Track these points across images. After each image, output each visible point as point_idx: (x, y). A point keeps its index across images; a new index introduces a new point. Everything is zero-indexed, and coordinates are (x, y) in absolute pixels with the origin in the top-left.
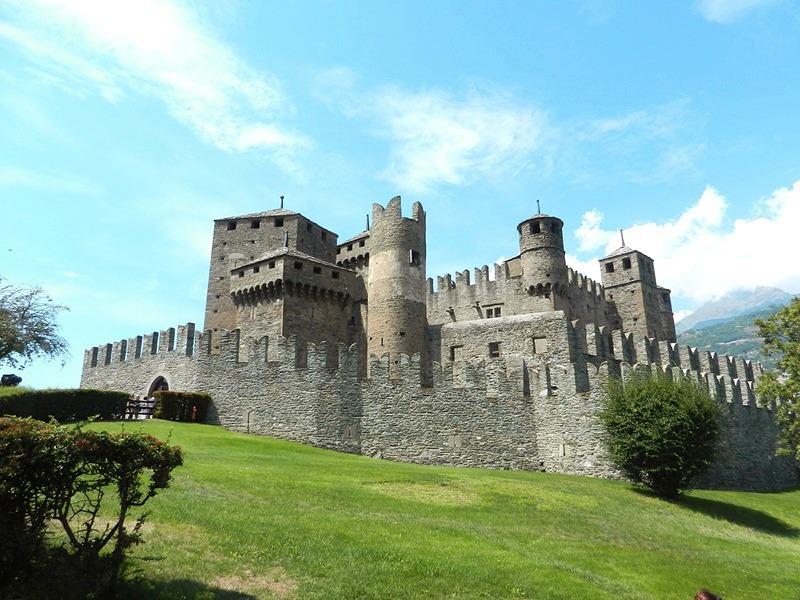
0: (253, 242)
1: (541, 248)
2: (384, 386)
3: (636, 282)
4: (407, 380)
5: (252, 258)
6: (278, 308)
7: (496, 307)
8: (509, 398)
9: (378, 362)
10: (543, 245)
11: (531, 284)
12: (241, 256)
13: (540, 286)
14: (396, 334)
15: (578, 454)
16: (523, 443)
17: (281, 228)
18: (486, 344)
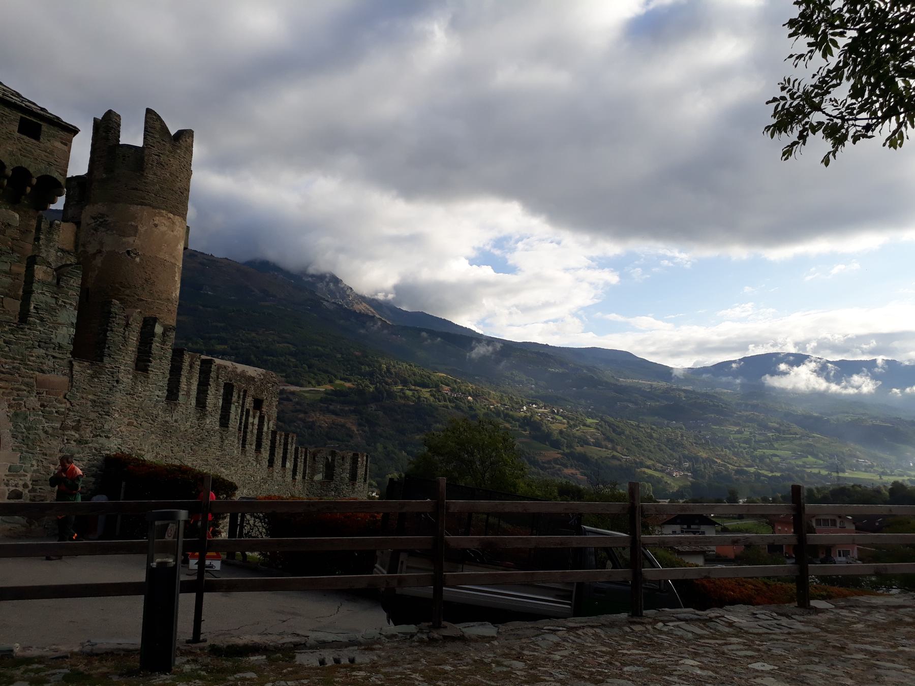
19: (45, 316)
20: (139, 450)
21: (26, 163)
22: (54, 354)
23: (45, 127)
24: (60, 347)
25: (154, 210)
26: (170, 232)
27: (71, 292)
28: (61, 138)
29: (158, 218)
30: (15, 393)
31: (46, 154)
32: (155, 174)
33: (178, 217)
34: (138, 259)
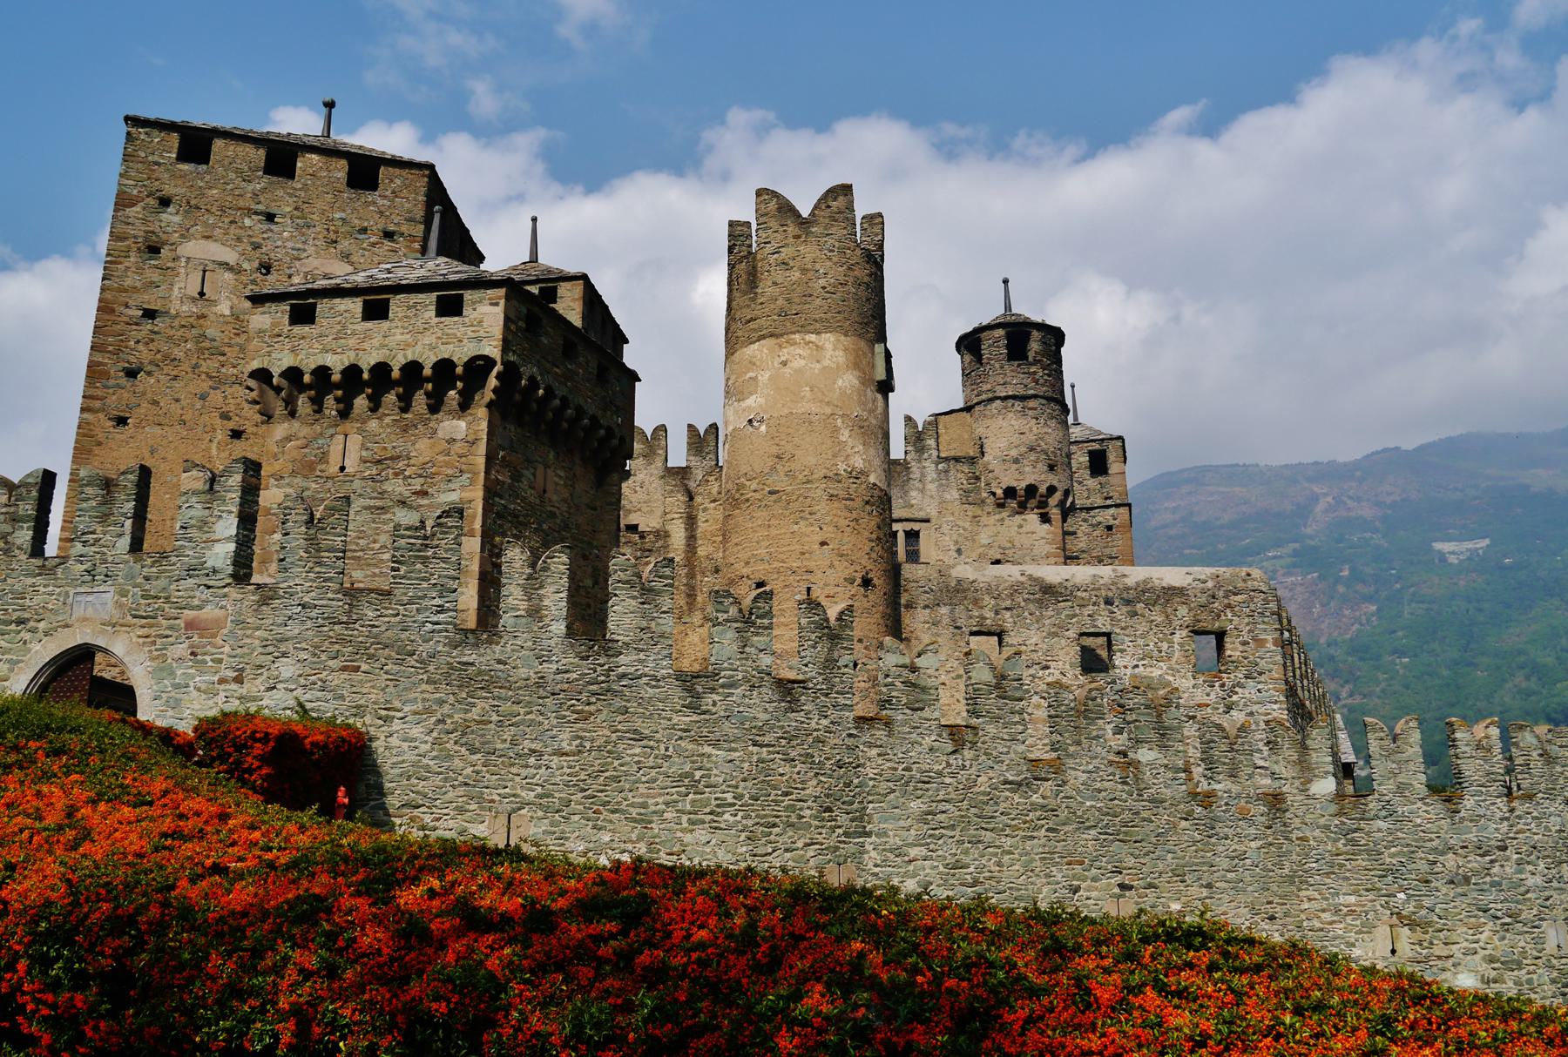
0: (270, 218)
1: (1035, 396)
2: (928, 741)
3: (1117, 506)
4: (991, 729)
5: (266, 268)
6: (457, 448)
7: (909, 526)
8: (1238, 796)
9: (914, 669)
10: (1042, 390)
11: (1008, 480)
12: (231, 256)
13: (1031, 490)
14: (851, 581)
15: (1438, 953)
16: (1272, 918)
17: (370, 196)
18: (1072, 634)
19: (194, 533)
20: (385, 709)
21: (445, 352)
22: (207, 582)
23: (468, 295)
24: (215, 571)
25: (778, 341)
26: (813, 366)
27: (230, 495)
28: (489, 299)
29: (785, 350)
30: (159, 641)
31: (474, 329)
32: (775, 284)
33: (829, 335)
34: (763, 428)
